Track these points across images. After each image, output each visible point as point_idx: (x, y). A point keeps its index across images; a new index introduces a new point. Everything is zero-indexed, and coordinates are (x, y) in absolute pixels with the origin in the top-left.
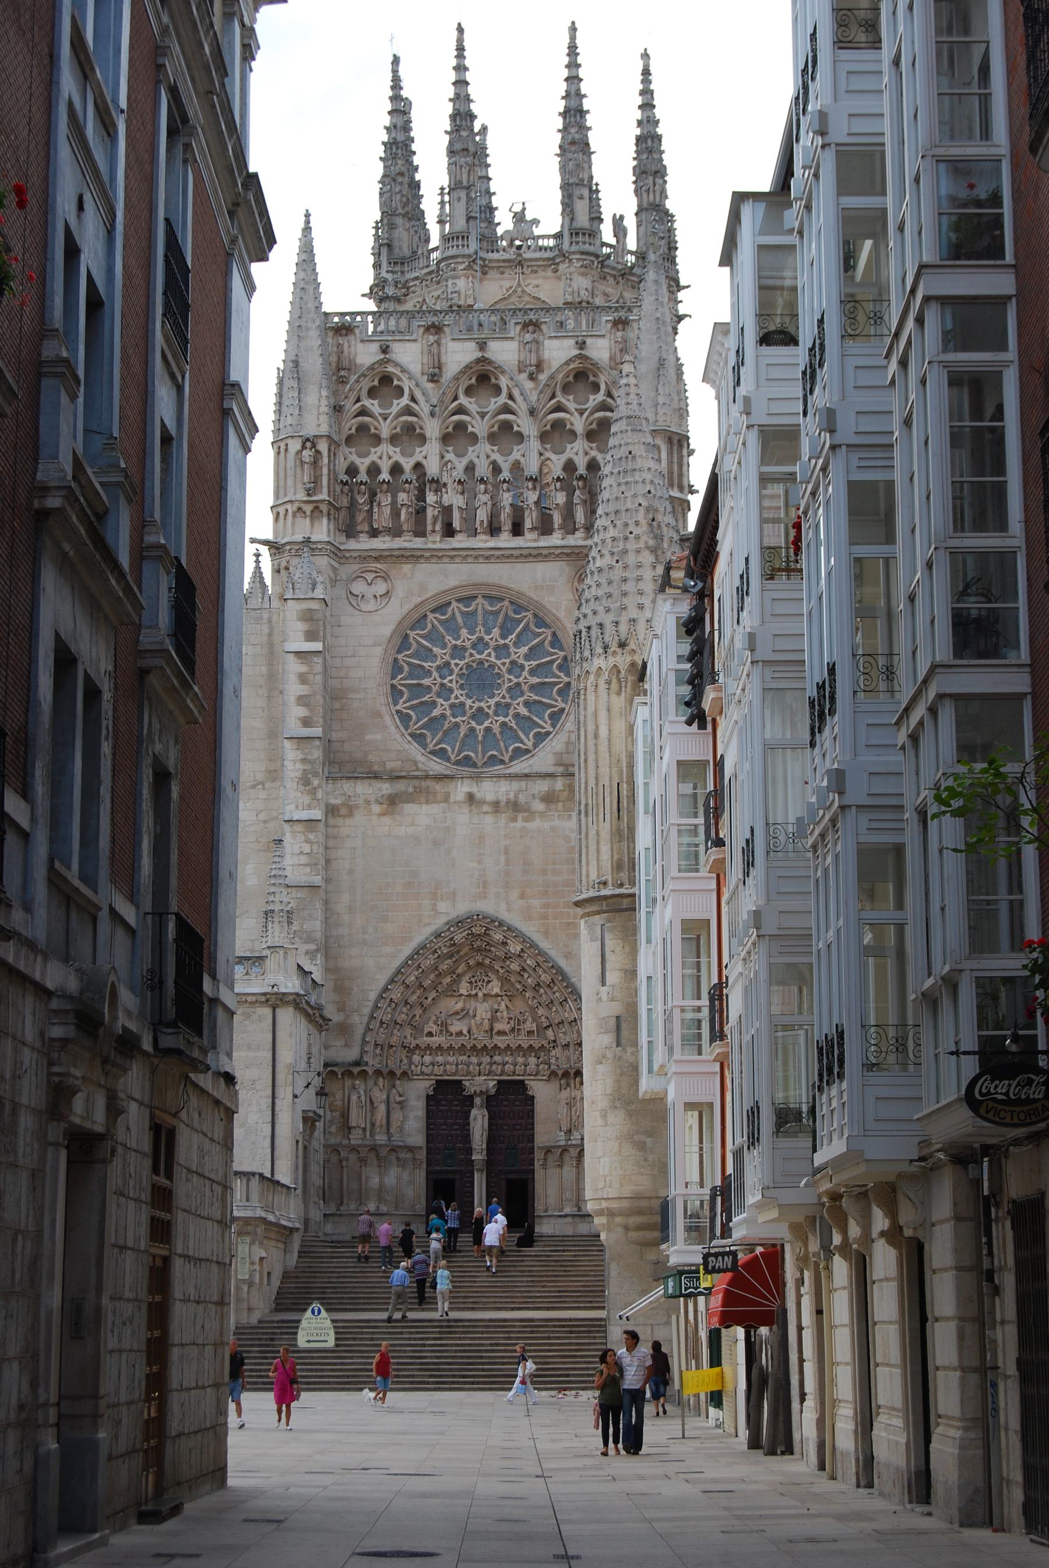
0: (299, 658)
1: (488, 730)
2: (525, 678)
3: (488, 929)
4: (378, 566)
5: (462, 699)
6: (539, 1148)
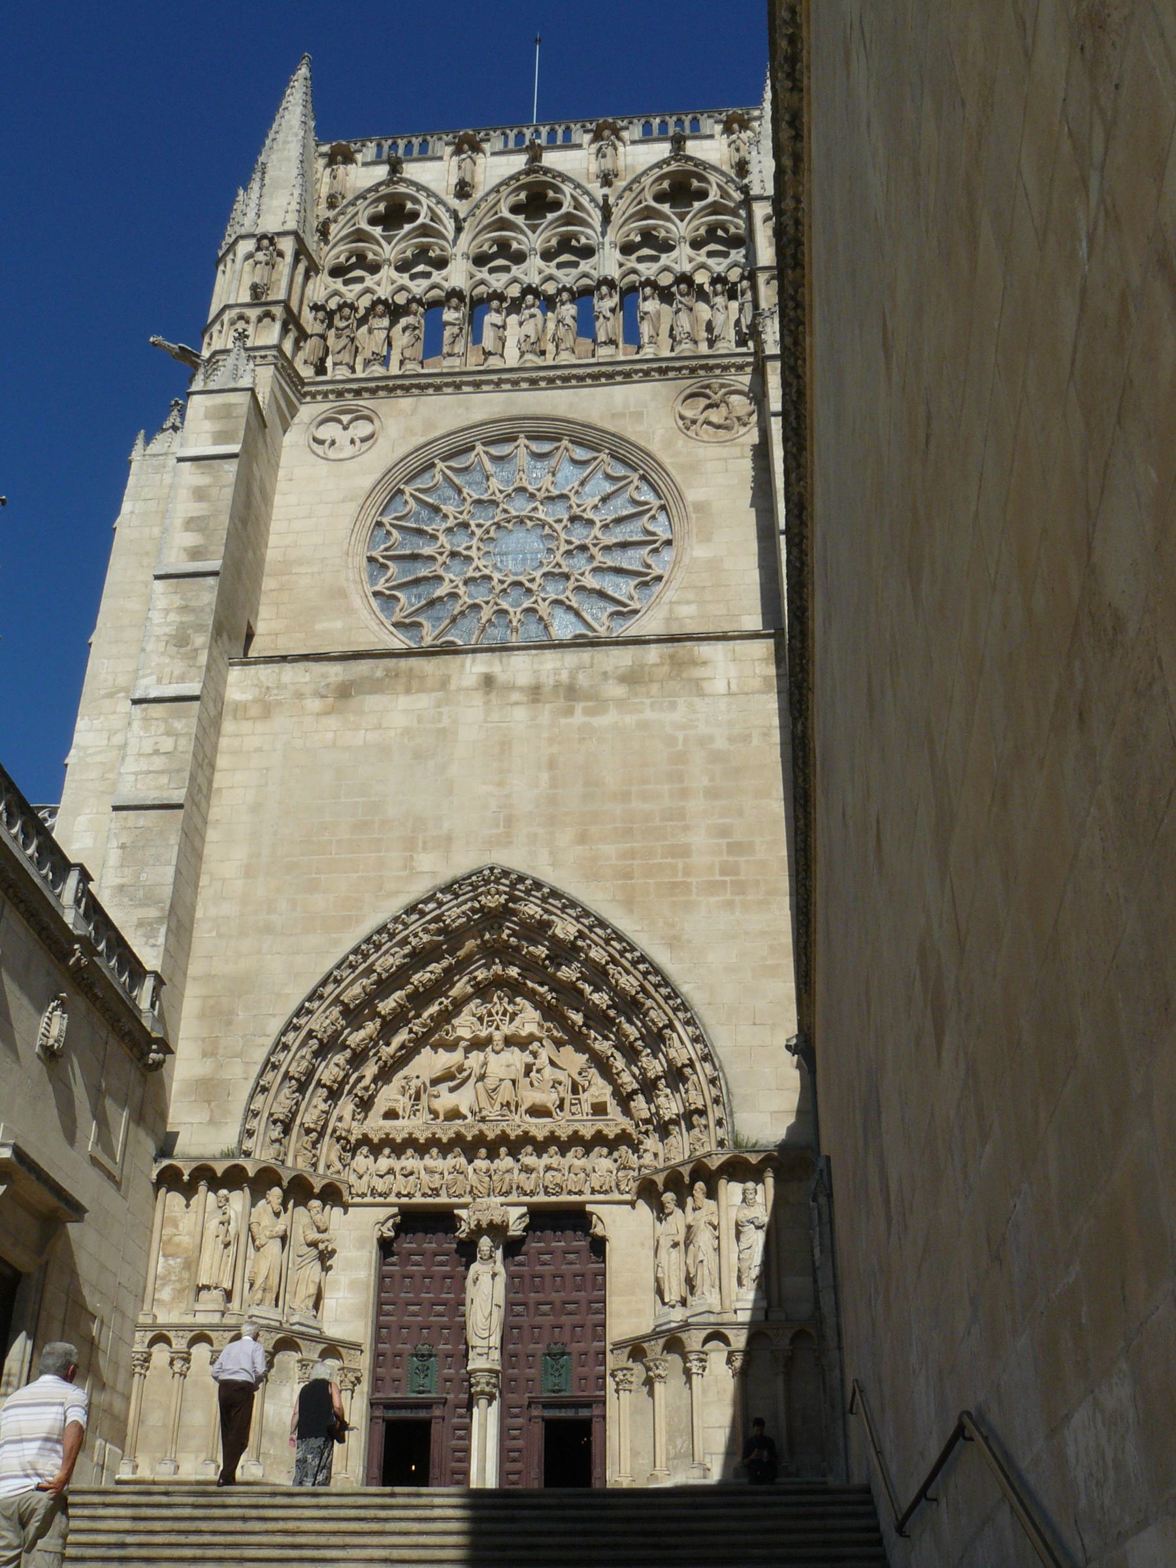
0: (198, 467)
1: (530, 611)
2: (596, 538)
3: (514, 899)
4: (361, 403)
5: (487, 572)
6: (618, 1346)
